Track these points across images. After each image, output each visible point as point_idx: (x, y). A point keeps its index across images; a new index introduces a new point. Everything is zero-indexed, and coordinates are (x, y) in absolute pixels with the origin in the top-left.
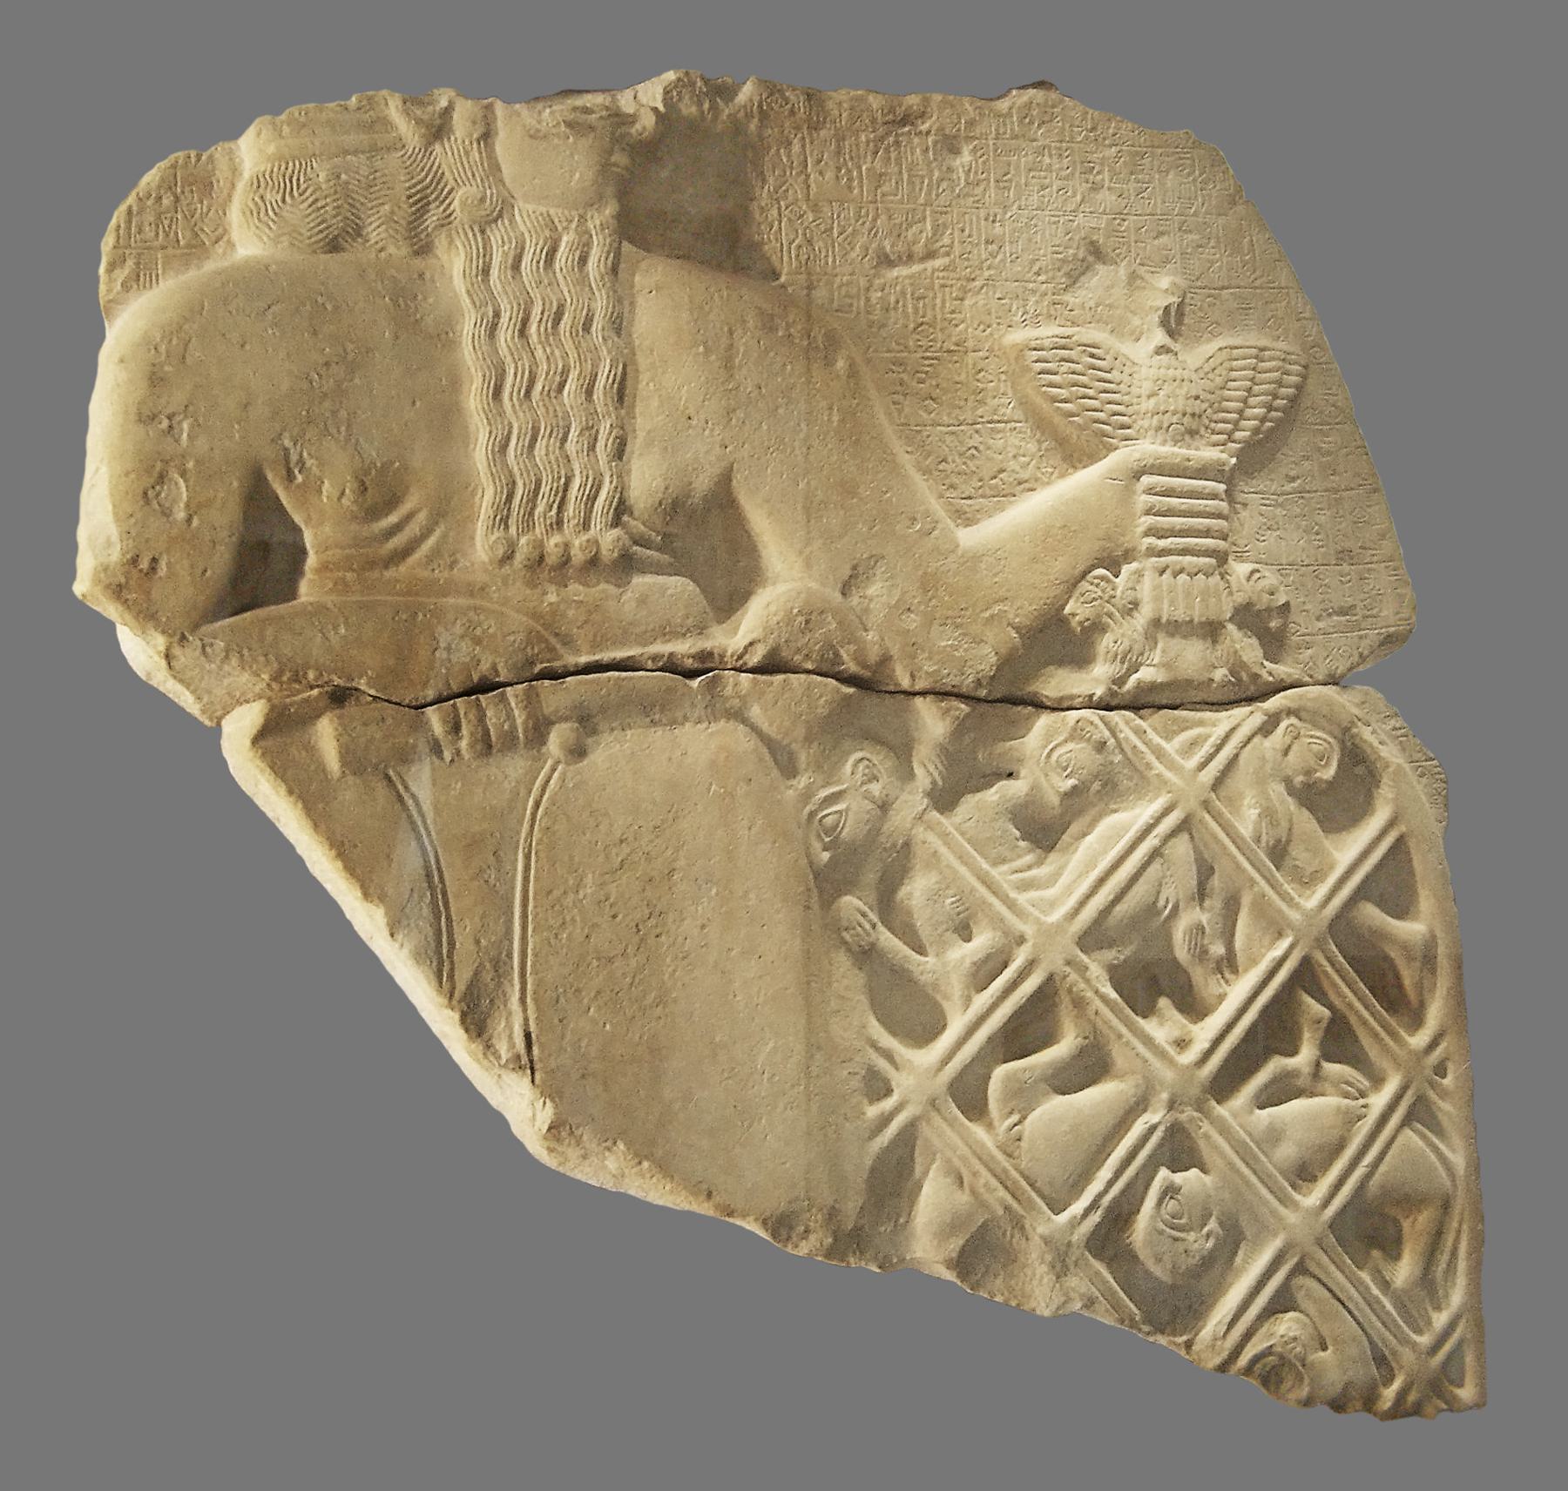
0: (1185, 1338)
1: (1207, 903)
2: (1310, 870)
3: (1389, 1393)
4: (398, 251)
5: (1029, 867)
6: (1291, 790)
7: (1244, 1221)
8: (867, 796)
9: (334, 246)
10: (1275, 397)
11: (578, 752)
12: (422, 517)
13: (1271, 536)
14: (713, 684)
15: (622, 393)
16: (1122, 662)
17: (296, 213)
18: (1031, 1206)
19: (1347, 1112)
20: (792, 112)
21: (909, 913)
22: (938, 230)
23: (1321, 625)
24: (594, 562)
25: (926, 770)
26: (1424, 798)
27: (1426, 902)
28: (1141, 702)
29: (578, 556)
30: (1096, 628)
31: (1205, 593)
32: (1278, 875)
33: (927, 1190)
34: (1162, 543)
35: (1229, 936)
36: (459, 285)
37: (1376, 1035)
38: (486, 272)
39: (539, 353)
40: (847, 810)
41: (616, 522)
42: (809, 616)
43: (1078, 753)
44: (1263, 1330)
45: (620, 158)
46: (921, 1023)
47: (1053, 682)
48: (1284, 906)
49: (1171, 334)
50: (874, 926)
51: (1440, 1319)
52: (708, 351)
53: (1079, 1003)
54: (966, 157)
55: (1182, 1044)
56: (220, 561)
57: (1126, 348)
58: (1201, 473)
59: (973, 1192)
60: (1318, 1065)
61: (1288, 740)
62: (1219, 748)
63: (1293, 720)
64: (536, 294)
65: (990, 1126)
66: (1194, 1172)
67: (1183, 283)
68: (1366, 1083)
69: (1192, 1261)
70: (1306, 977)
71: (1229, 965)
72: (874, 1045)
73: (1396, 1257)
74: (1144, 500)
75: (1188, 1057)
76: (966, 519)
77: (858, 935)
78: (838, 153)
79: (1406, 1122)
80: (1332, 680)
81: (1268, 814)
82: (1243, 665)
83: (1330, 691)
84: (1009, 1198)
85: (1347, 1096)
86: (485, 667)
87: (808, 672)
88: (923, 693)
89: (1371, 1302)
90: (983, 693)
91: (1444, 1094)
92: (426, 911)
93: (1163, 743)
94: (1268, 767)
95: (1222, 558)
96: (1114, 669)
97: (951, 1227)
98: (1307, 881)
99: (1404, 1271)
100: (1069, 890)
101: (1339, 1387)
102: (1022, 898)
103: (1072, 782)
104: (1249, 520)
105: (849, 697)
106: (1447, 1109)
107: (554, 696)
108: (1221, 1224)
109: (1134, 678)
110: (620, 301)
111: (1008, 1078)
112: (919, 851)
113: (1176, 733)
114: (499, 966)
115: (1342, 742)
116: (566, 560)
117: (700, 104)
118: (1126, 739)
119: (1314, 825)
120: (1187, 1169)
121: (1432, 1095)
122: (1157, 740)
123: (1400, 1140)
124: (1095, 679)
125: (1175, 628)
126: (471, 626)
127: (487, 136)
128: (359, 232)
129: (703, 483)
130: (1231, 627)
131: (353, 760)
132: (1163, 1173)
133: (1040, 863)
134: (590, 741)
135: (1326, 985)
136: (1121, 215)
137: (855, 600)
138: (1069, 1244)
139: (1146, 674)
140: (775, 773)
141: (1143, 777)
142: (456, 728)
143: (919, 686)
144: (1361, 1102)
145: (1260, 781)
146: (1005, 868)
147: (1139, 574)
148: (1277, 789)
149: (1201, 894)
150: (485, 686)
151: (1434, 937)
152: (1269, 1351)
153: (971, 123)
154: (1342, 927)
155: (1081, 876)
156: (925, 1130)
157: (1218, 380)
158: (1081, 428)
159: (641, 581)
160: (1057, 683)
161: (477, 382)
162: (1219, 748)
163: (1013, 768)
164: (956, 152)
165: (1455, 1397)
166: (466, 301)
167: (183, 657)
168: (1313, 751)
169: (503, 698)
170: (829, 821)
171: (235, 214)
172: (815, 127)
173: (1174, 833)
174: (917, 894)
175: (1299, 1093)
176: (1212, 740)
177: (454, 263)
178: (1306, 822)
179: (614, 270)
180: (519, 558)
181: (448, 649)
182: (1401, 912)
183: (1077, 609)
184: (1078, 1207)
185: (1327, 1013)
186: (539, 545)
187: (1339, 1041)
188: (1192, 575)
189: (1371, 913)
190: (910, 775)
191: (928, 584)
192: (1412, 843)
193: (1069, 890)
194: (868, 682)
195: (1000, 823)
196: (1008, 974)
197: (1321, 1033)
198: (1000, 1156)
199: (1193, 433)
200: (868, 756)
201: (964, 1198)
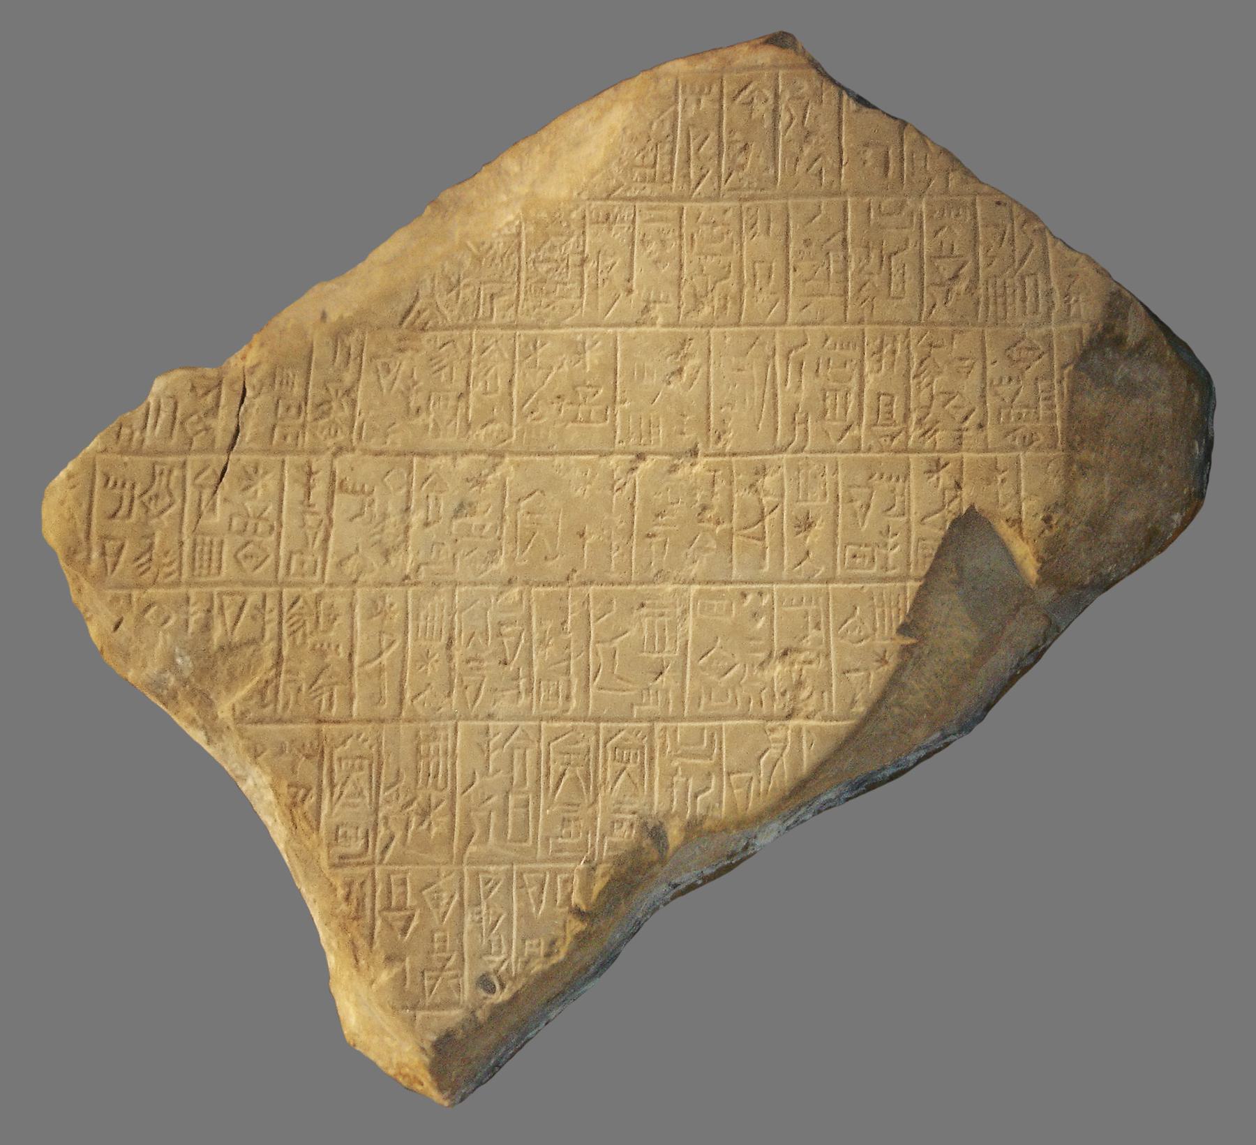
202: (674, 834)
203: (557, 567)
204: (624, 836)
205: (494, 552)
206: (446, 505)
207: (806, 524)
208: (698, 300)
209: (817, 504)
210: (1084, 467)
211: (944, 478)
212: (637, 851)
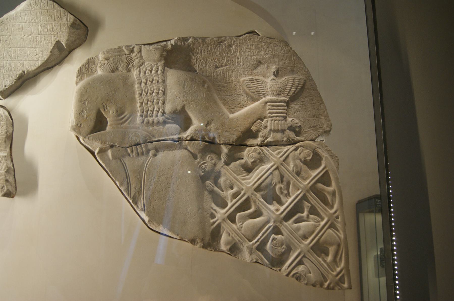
0: (279, 269)
2: (305, 177)
3: (326, 284)
4: (124, 71)
5: (245, 176)
7: (292, 246)
8: (211, 163)
9: (113, 71)
10: (298, 87)
11: (155, 155)
12: (128, 116)
13: (298, 113)
14: (181, 142)
15: (164, 93)
17: (107, 67)
18: (245, 240)
19: (315, 225)
20: (199, 43)
21: (220, 184)
22: (227, 61)
24: (158, 122)
26: (332, 162)
27: (333, 184)
29: (155, 121)
30: (258, 131)
31: (281, 124)
32: (298, 178)
33: (223, 236)
34: (272, 115)
35: (288, 189)
36: (135, 77)
38: (140, 74)
39: (149, 87)
41: (163, 115)
42: (199, 130)
43: (255, 155)
45: (165, 53)
46: (223, 205)
48: (299, 184)
49: (276, 76)
51: (338, 269)
52: (180, 85)
53: (255, 202)
54: (234, 47)
55: (277, 210)
56: (91, 124)
57: (265, 80)
58: (280, 102)
59: (232, 237)
62: (285, 153)
63: (302, 148)
64: (148, 77)
65: (236, 225)
66: (280, 236)
67: (278, 67)
68: (319, 219)
69: (280, 253)
70: (304, 198)
71: (288, 195)
72: (212, 208)
73: (327, 255)
74: (268, 107)
75: (278, 213)
76: (233, 112)
78: (208, 49)
79: (329, 227)
80: (311, 140)
81: (296, 166)
82: (290, 137)
83: (311, 142)
84: (239, 238)
85: (315, 222)
86: (138, 141)
88: (222, 144)
89: (322, 265)
91: (338, 222)
92: (126, 183)
93: (273, 153)
94: (296, 157)
95: (285, 118)
96: (262, 139)
97: (227, 243)
98: (305, 179)
99: (330, 258)
100: (253, 180)
101: (314, 282)
102: (243, 182)
103: (253, 160)
104: (292, 110)
105: (206, 145)
106: (339, 226)
107: (150, 146)
108: (286, 246)
110: (164, 77)
111: (239, 216)
112: (222, 173)
113: (276, 151)
114: (139, 193)
115: (313, 152)
116: (153, 122)
117: (181, 43)
119: (307, 168)
120: (278, 235)
121: (335, 223)
123: (327, 232)
124: (259, 140)
125: (275, 131)
126: (136, 134)
127: (140, 51)
128: (117, 69)
129: (179, 108)
130: (287, 131)
131: (114, 157)
133: (248, 175)
134: (157, 153)
135: (310, 200)
136: (266, 55)
137: (208, 128)
138: (252, 248)
139: (269, 140)
140: (193, 158)
141: (269, 159)
142: (132, 151)
143: (221, 142)
145: (294, 160)
146: (240, 176)
147: (267, 121)
148: (298, 162)
149: (282, 181)
150: (138, 144)
151: (335, 190)
152: (297, 273)
153: (234, 41)
154: (313, 188)
155: (256, 177)
157: (285, 84)
158: (255, 94)
159: (167, 126)
161: (138, 93)
162: (285, 153)
163: (242, 157)
164: (232, 47)
165: (343, 286)
166: (136, 79)
167: (86, 140)
168: (306, 154)
169: (141, 146)
170: (203, 167)
171: (98, 67)
172: (204, 45)
173: (275, 169)
177: (134, 73)
178: (305, 167)
179: (163, 72)
180: (145, 122)
181: (132, 138)
182: (329, 185)
183: (254, 128)
184: (254, 241)
185: (310, 205)
186: (148, 120)
187: (313, 211)
188: (278, 121)
189: (320, 185)
190: (221, 159)
191: (223, 124)
192: (330, 172)
193: (253, 180)
194: (212, 142)
196: (240, 196)
197: (308, 209)
198: (238, 230)
199: (279, 94)
201: (230, 238)
202: (26, 72)
203: (15, 46)
204: (20, 72)
205: (9, 45)
206: (4, 40)
207: (41, 42)
208: (32, 20)
209: (42, 40)
210: (71, 36)
211: (56, 37)
212: (22, 74)
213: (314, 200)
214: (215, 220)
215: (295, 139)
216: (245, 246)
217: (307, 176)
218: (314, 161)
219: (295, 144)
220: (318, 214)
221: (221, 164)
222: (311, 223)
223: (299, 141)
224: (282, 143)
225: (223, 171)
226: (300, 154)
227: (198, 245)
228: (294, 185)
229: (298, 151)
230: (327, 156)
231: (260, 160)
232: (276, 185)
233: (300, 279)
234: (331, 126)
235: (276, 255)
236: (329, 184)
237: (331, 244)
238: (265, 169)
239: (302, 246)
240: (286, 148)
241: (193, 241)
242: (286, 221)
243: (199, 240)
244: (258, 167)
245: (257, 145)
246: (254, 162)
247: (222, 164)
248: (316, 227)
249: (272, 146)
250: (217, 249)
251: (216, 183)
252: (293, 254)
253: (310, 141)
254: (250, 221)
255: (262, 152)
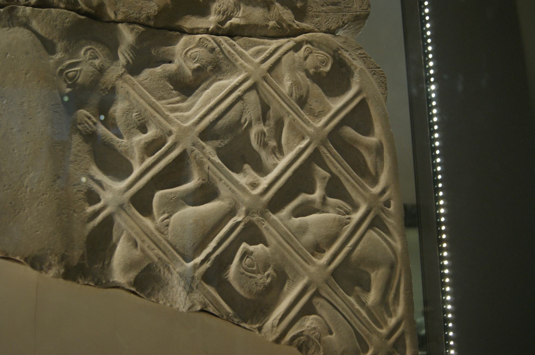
0: (257, 325)
1: (267, 122)
2: (317, 111)
5: (178, 102)
6: (308, 75)
14: (12, 9)
16: (223, 15)
18: (174, 259)
19: (340, 220)
21: (114, 119)
23: (324, 8)
25: (124, 56)
26: (374, 83)
27: (377, 128)
28: (233, 33)
32: (302, 112)
35: (278, 139)
37: (354, 186)
40: (81, 70)
43: (200, 52)
44: (298, 324)
47: (189, 22)
48: (304, 125)
50: (95, 124)
51: (392, 322)
53: (200, 164)
55: (254, 185)
59: (143, 250)
60: (324, 199)
61: (306, 53)
62: (271, 54)
63: (309, 46)
65: (153, 219)
66: (260, 246)
69: (260, 288)
70: (316, 157)
71: (279, 151)
73: (367, 289)
77: (85, 127)
79: (371, 226)
80: (329, 31)
81: (296, 84)
82: (283, 20)
84: (161, 254)
85: (339, 213)
87: (62, 8)
88: (122, 22)
89: (356, 313)
90: (152, 23)
91: (388, 214)
93: (244, 51)
94: (297, 64)
96: (220, 18)
97: (129, 267)
98: (317, 116)
99: (372, 297)
100: (196, 113)
102: (172, 115)
103: (197, 65)
108: (275, 270)
109: (228, 23)
111: (161, 197)
113: (251, 47)
115: (334, 57)
118: (225, 48)
119: (320, 91)
122: (240, 49)
124: (211, 21)
132: (244, 245)
133: (183, 101)
138: (193, 278)
140: (43, 52)
141: (234, 66)
143: (120, 17)
144: (347, 216)
145: (292, 70)
148: (301, 75)
151: (381, 143)
152: (301, 334)
154: (334, 136)
155: (203, 106)
156: (118, 220)
160: (191, 22)
162: (271, 54)
163: (169, 58)
168: (318, 59)
170: (70, 74)
174: (118, 110)
175: (316, 211)
176: (268, 51)
178: (316, 90)
184: (198, 260)
185: (328, 175)
187: (335, 188)
189: (349, 131)
190: (116, 58)
192: (369, 103)
193: (196, 113)
195: (162, 82)
196: (163, 149)
197: (325, 185)
198: (156, 233)
200: (94, 48)
201: (137, 253)
213: (338, 165)
214: (98, 206)
215: (295, 26)
216: (179, 273)
217: (321, 109)
218: (335, 79)
219: (295, 36)
220: (345, 196)
221: (116, 70)
222: (331, 215)
223: (303, 31)
224: (263, 33)
225: (122, 87)
226: (306, 58)
227: (52, 272)
228: (293, 127)
229: (302, 52)
230: (363, 67)
231: (214, 67)
232: (250, 125)
233: (308, 349)
234: (369, 6)
235: (250, 292)
236: (368, 131)
237: (375, 265)
238: (224, 87)
239: (312, 269)
240: (274, 44)
241: (36, 262)
242: (274, 212)
243: (53, 259)
244: (208, 82)
245: (207, 31)
246: (198, 69)
247: (121, 70)
248: (342, 224)
249: (243, 36)
250: (103, 282)
251: (104, 108)
252: (290, 289)
253: (325, 32)
254: (189, 211)
255: (218, 49)
